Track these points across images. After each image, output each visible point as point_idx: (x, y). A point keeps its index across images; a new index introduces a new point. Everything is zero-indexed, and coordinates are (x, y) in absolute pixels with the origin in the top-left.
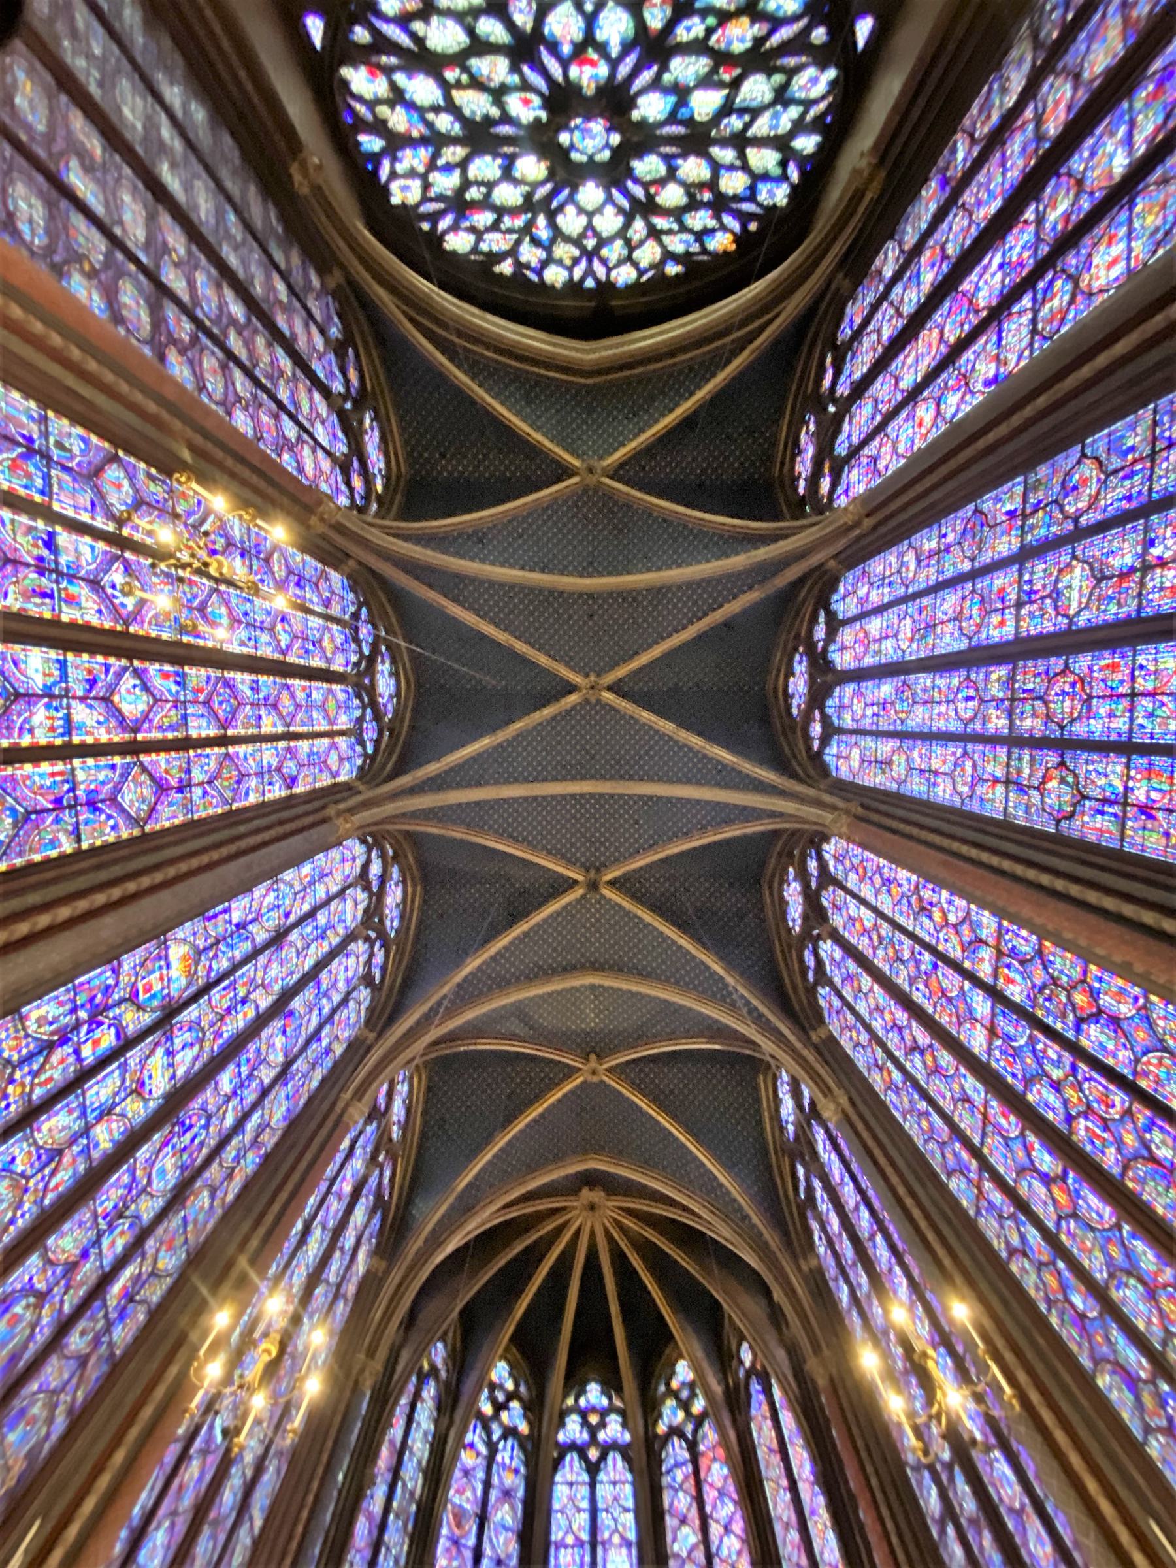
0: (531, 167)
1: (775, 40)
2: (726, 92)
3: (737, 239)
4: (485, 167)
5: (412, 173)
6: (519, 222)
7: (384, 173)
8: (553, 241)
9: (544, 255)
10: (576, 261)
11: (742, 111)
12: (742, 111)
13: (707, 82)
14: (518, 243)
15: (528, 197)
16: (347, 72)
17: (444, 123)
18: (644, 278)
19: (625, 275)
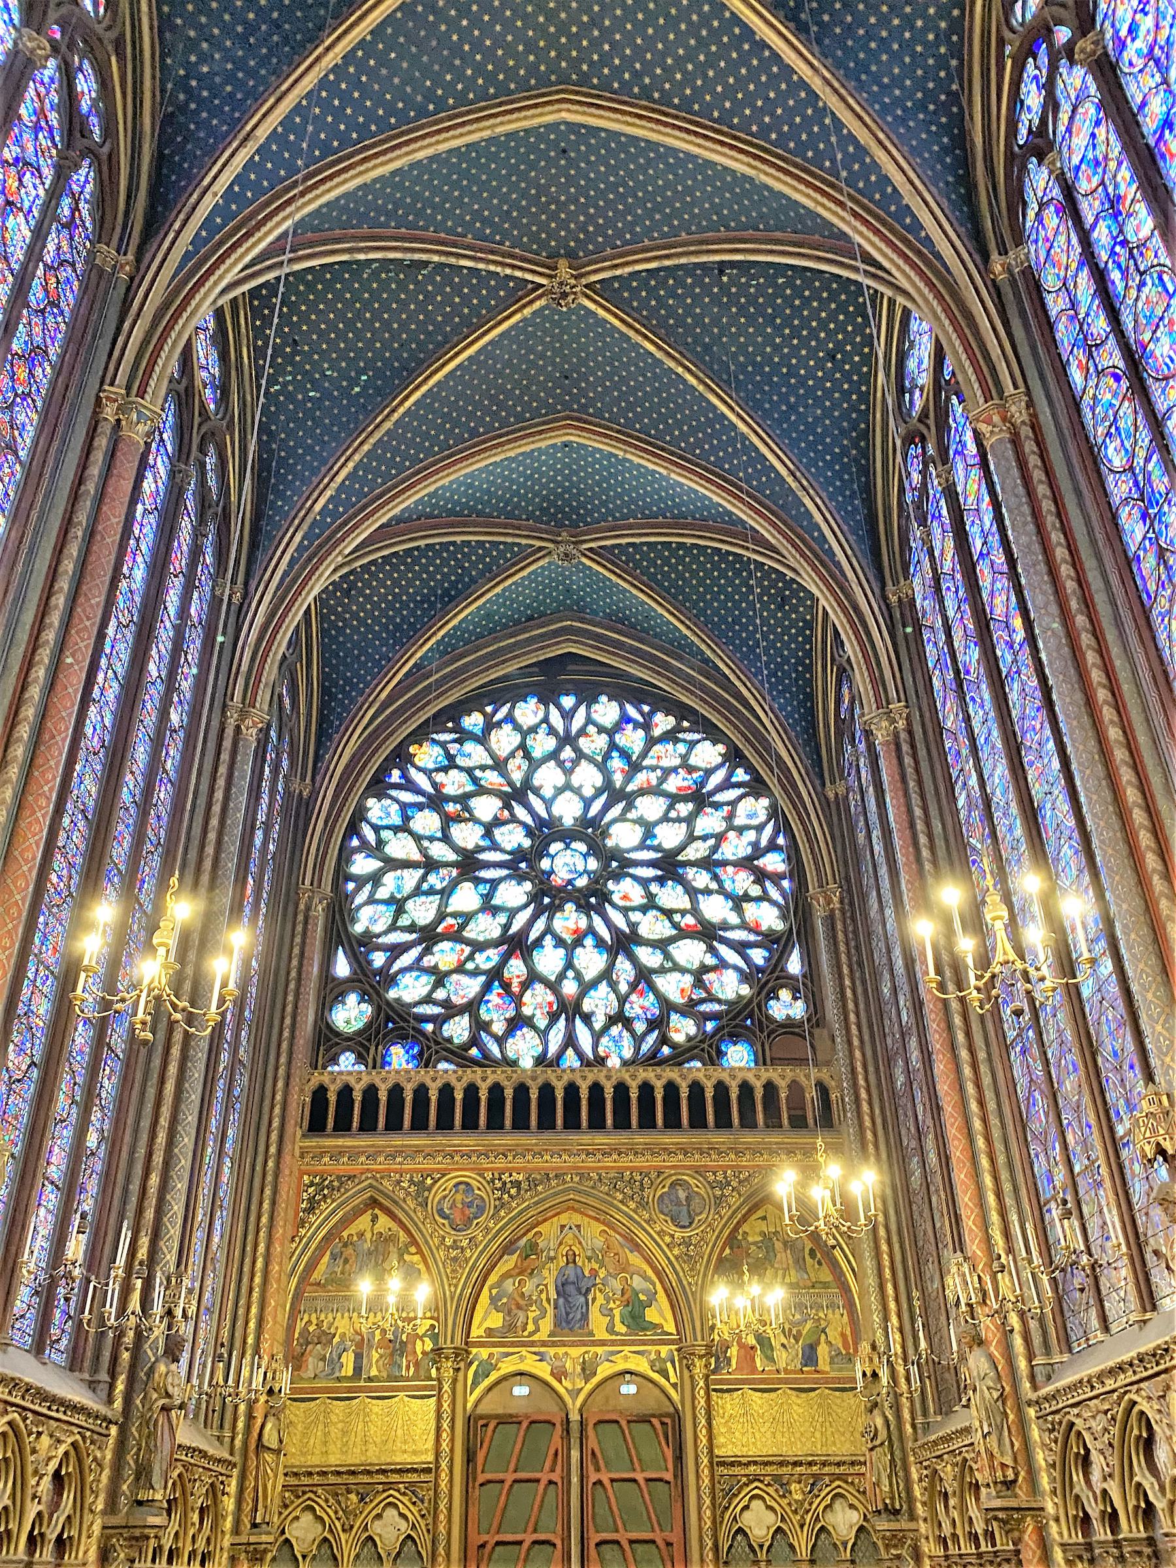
0: (624, 836)
1: (415, 953)
3: (410, 759)
4: (670, 836)
5: (741, 830)
6: (641, 779)
7: (769, 830)
8: (607, 756)
10: (582, 732)
11: (431, 892)
12: (431, 892)
13: (468, 917)
14: (644, 754)
15: (630, 806)
16: (779, 926)
17: (701, 879)
18: (504, 710)
19: (528, 712)
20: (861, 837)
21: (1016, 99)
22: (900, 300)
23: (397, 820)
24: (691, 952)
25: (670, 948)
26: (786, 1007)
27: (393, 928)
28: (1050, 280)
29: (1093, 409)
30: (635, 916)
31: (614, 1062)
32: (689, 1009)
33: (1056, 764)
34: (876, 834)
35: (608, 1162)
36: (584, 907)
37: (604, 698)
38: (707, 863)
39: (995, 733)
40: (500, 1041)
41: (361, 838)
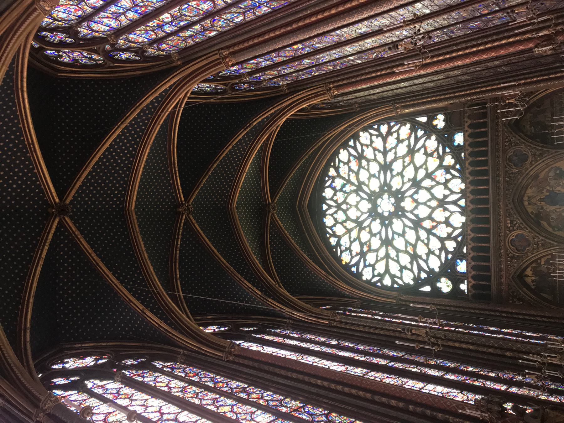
0: (375, 185)
1: (421, 262)
2: (404, 249)
3: (347, 264)
4: (374, 168)
5: (372, 142)
6: (353, 178)
7: (371, 131)
8: (345, 192)
9: (338, 188)
10: (336, 202)
11: (397, 256)
12: (397, 256)
13: (407, 242)
15: (363, 183)
16: (408, 126)
18: (328, 230)
19: (328, 221)
20: (374, 97)
21: (128, 61)
22: (188, 95)
23: (370, 269)
24: (419, 158)
25: (418, 166)
26: (440, 122)
27: (411, 270)
28: (183, 45)
29: (224, 27)
30: (406, 180)
31: (463, 186)
32: (441, 158)
33: (345, 30)
34: (372, 92)
35: (502, 187)
36: (403, 199)
37: (324, 194)
38: (385, 153)
39: (334, 51)
40: (455, 229)
41: (378, 281)
